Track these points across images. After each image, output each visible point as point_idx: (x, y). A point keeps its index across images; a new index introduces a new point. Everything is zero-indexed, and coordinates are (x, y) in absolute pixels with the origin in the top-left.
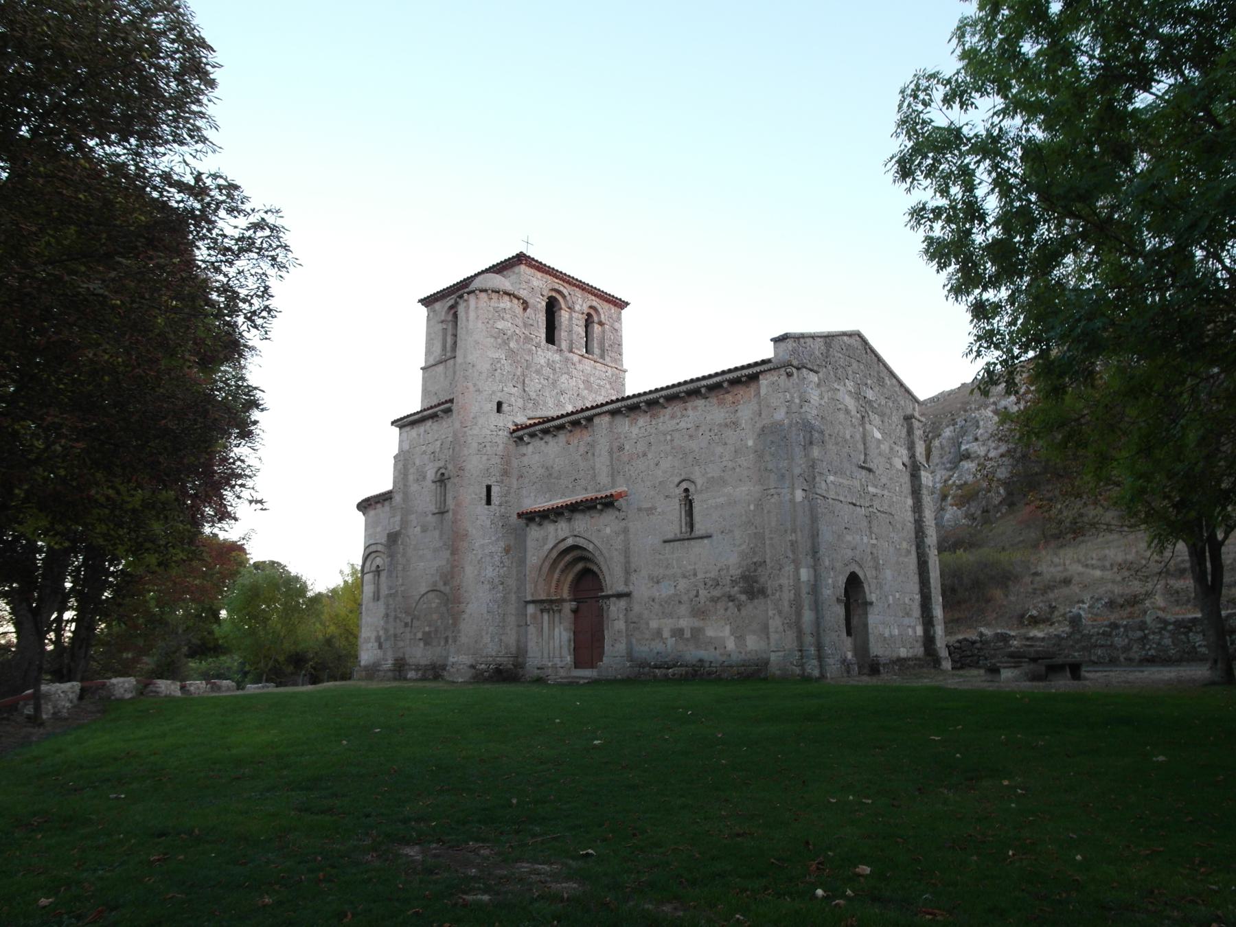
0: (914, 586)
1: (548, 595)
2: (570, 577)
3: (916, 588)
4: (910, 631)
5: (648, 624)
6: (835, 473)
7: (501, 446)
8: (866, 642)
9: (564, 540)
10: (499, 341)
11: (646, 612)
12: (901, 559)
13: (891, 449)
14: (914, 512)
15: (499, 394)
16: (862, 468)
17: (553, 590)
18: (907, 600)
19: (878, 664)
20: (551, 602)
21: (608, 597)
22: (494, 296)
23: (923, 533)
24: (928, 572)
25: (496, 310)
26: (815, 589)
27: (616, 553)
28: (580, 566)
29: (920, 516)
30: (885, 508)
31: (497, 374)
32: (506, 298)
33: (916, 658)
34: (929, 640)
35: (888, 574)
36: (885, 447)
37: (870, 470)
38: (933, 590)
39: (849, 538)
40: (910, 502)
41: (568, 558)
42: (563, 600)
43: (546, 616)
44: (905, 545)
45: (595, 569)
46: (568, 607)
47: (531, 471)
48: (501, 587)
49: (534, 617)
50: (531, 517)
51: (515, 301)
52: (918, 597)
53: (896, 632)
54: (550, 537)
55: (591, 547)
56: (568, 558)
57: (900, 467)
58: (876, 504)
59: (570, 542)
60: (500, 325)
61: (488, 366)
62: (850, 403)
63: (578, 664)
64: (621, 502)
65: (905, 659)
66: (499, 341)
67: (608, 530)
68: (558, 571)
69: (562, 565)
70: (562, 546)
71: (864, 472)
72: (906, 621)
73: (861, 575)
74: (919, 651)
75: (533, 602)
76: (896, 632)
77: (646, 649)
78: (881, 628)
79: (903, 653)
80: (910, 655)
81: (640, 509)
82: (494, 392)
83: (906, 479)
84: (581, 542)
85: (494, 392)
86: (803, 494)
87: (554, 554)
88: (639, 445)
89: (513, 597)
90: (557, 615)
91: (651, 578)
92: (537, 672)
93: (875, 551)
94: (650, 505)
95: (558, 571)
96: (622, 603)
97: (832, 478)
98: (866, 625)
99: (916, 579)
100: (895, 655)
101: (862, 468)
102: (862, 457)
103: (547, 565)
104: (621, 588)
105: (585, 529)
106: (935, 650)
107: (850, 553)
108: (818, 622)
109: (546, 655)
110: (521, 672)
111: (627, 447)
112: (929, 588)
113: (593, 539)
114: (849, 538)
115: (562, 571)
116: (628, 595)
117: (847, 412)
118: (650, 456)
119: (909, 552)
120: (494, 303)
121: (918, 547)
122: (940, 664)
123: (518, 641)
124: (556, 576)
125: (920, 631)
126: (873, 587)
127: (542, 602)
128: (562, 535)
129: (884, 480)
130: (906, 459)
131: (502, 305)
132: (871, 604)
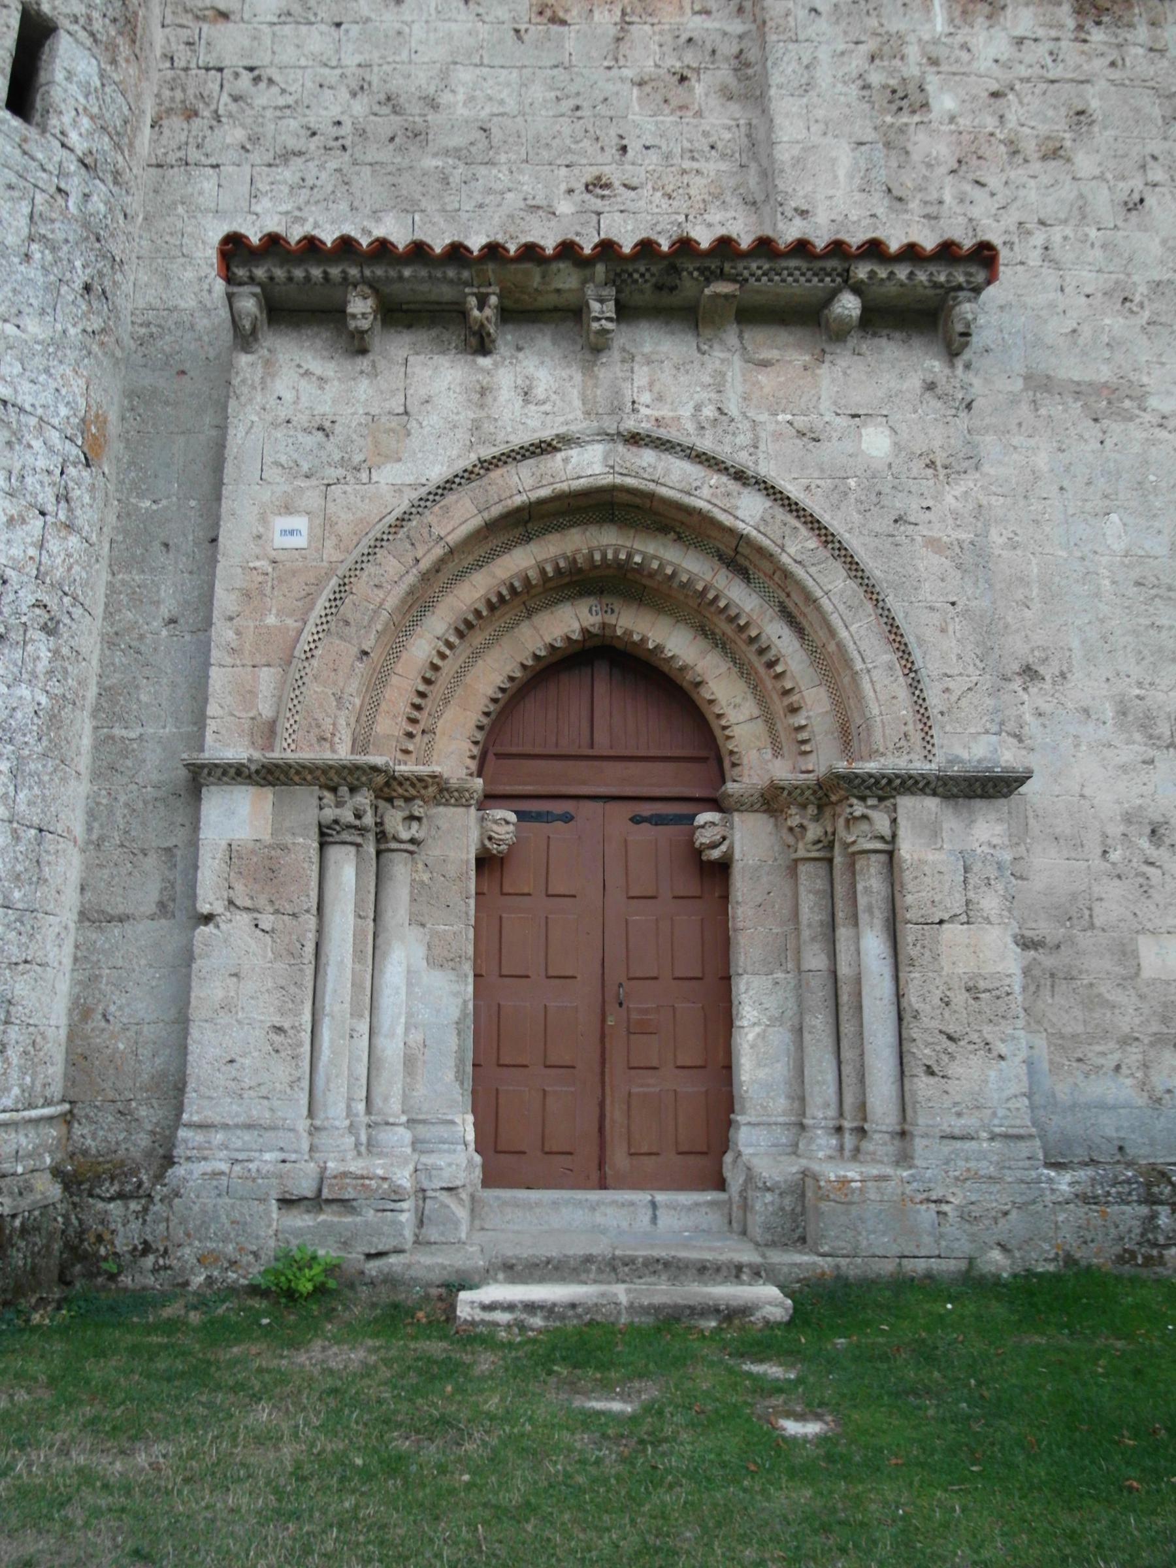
1: (360, 744)
2: (493, 671)
5: (1126, 953)
9: (543, 448)
11: (1113, 891)
17: (390, 725)
20: (388, 787)
21: (888, 788)
27: (930, 563)
28: (567, 622)
41: (521, 561)
42: (440, 791)
43: (346, 870)
45: (677, 644)
46: (458, 835)
47: (263, 97)
48: (42, 647)
49: (260, 868)
50: (298, 289)
54: (433, 420)
55: (748, 512)
56: (521, 561)
59: (588, 466)
63: (506, 1158)
64: (990, 313)
67: (876, 442)
68: (438, 624)
69: (474, 590)
70: (525, 484)
75: (271, 776)
77: (1123, 1090)
81: (1040, 384)
84: (673, 478)
87: (462, 516)
88: (1014, 112)
89: (83, 733)
90: (401, 870)
91: (1135, 718)
92: (275, 1230)
94: (1105, 374)
95: (438, 624)
96: (986, 828)
103: (393, 575)
104: (970, 747)
105: (693, 406)
109: (335, 1110)
110: (122, 1225)
111: (944, 102)
113: (767, 469)
115: (465, 628)
116: (992, 787)
118: (1085, 162)
123: (81, 1013)
124: (421, 648)
127: (335, 779)
128: (518, 424)
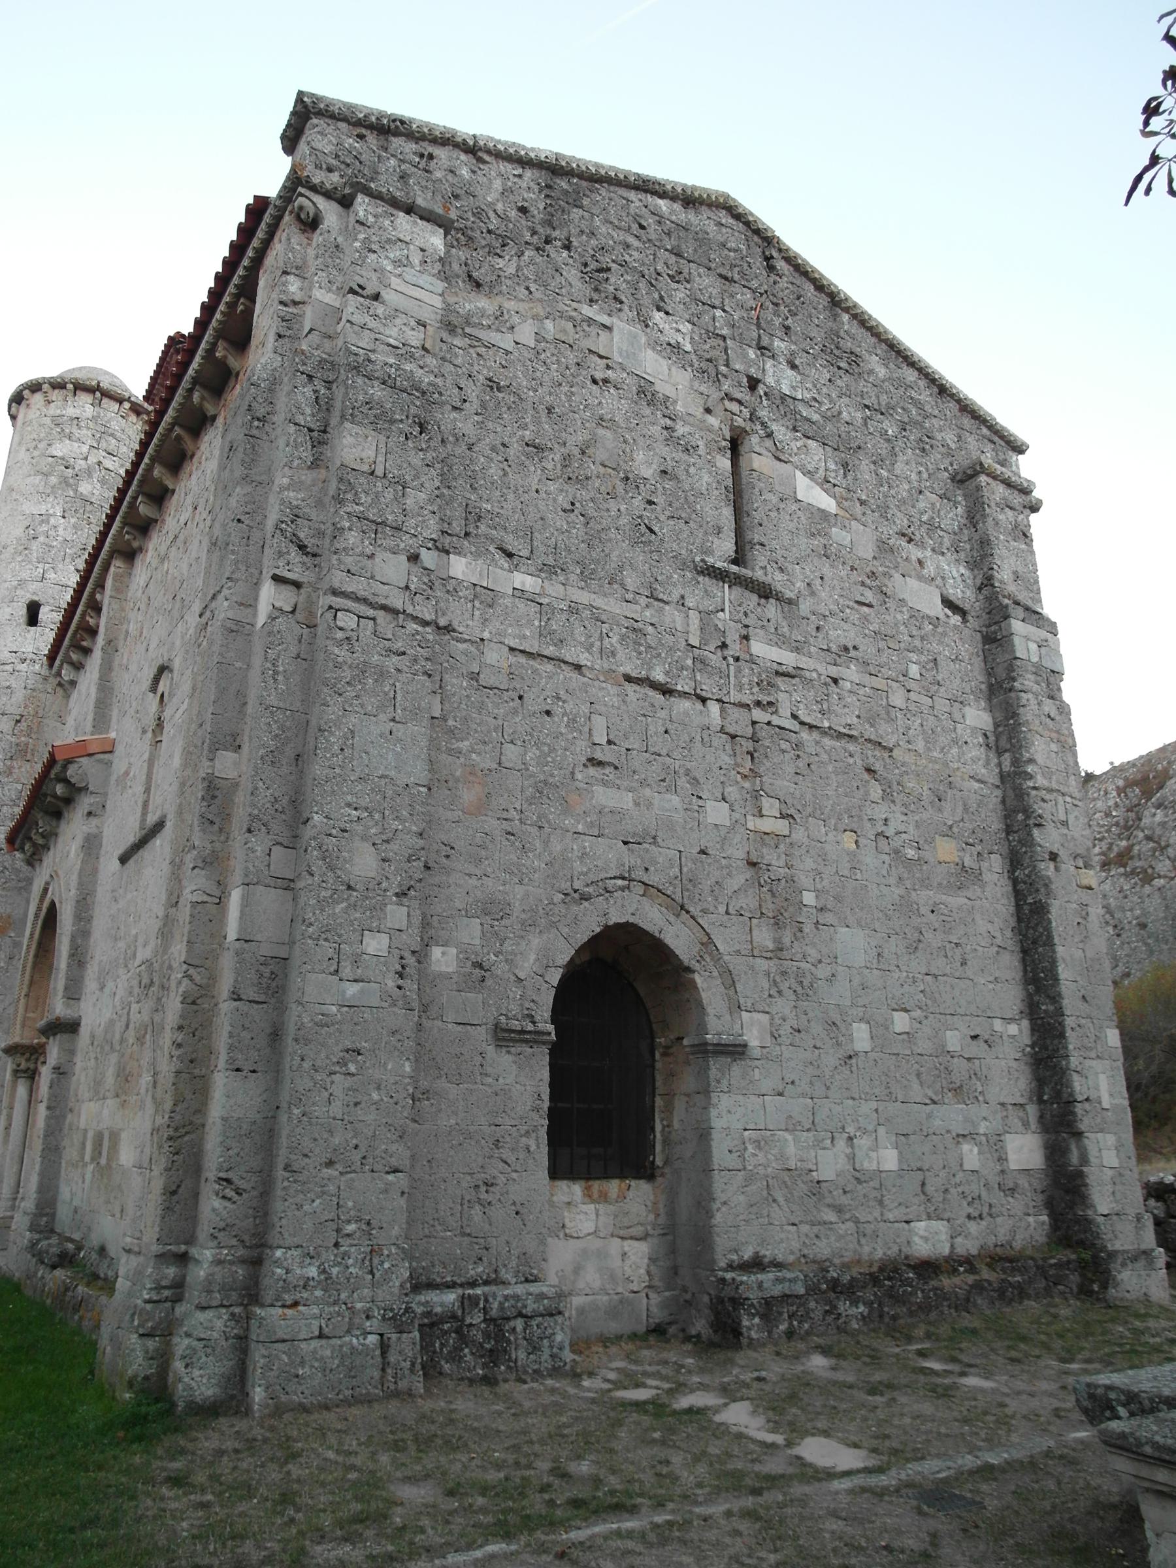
0: (998, 988)
3: (1011, 997)
4: (971, 1155)
6: (548, 570)
7: (19, 695)
8: (704, 1203)
10: (53, 480)
12: (924, 897)
13: (884, 548)
14: (1000, 753)
15: (34, 586)
16: (719, 575)
18: (954, 1040)
19: (738, 1302)
22: (56, 395)
23: (1027, 812)
24: (1049, 943)
25: (57, 422)
26: (273, 979)
29: (1016, 762)
30: (845, 717)
31: (35, 546)
32: (85, 399)
33: (998, 1258)
34: (1064, 1187)
35: (852, 943)
36: (859, 539)
37: (765, 592)
38: (1070, 1004)
39: (604, 797)
40: (977, 717)
44: (946, 850)
51: (115, 406)
52: (1018, 1032)
53: (889, 1159)
57: (936, 609)
58: (787, 698)
60: (59, 449)
61: (19, 531)
62: (675, 383)
65: (927, 1268)
66: (53, 480)
71: (727, 594)
72: (951, 1115)
73: (679, 939)
74: (1024, 1225)
76: (889, 1159)
78: (792, 1148)
79: (928, 1238)
80: (968, 1246)
82: (22, 583)
83: (959, 647)
85: (22, 583)
86: (286, 598)
93: (773, 858)
97: (525, 581)
98: (704, 1135)
99: (1009, 966)
100: (877, 1251)
101: (719, 575)
102: (725, 546)
106: (1086, 1223)
107: (610, 856)
108: (265, 1133)
112: (1056, 999)
114: (604, 797)
117: (646, 393)
119: (965, 876)
120: (53, 410)
121: (1014, 861)
122: (1106, 1279)
125: (1025, 1150)
126: (750, 987)
129: (839, 634)
130: (960, 592)
131: (71, 411)
132: (736, 1051)
